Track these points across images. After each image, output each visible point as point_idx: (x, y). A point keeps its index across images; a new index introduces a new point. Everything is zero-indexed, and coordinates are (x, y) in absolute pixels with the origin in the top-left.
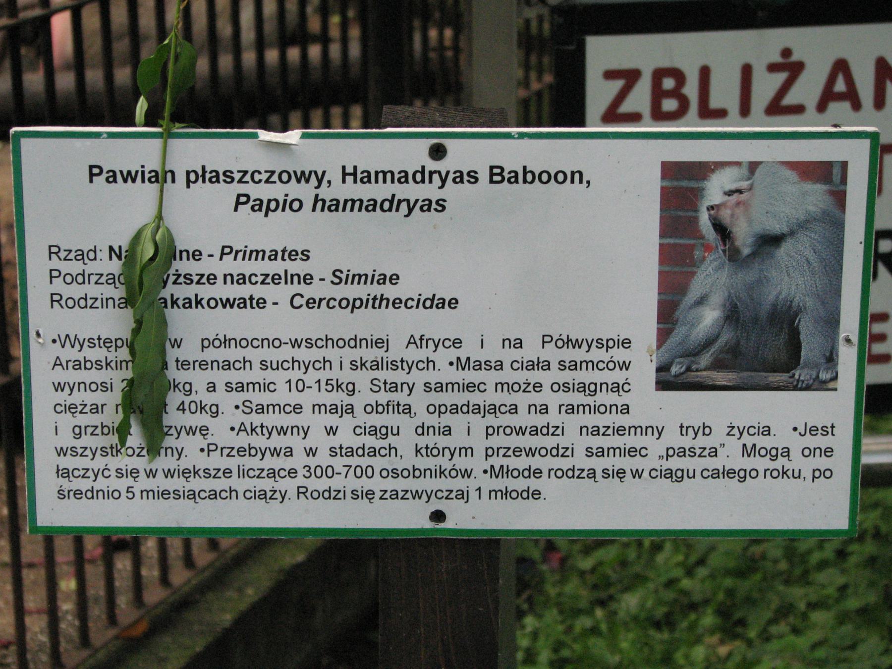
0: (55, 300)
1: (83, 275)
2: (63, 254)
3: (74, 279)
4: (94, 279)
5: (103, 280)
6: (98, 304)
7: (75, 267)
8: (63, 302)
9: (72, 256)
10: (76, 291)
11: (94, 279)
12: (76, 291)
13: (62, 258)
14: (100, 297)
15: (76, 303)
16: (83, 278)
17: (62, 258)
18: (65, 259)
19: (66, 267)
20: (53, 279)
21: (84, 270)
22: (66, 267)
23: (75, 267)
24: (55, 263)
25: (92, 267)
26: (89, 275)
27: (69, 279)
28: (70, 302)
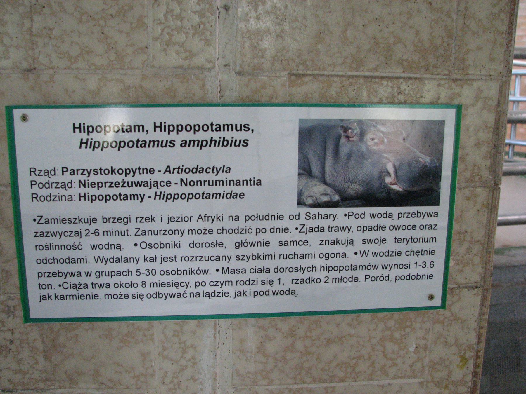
0: (34, 197)
1: (49, 184)
2: (37, 172)
3: (44, 186)
4: (54, 185)
5: (59, 186)
6: (57, 199)
7: (44, 179)
8: (38, 198)
9: (42, 173)
10: (45, 192)
11: (54, 185)
12: (45, 192)
13: (37, 174)
14: (58, 195)
15: (45, 198)
16: (49, 185)
17: (37, 174)
18: (39, 175)
19: (39, 179)
20: (33, 186)
21: (49, 181)
22: (39, 179)
23: (44, 179)
24: (34, 177)
25: (53, 179)
26: (52, 183)
27: (41, 186)
28: (42, 199)
